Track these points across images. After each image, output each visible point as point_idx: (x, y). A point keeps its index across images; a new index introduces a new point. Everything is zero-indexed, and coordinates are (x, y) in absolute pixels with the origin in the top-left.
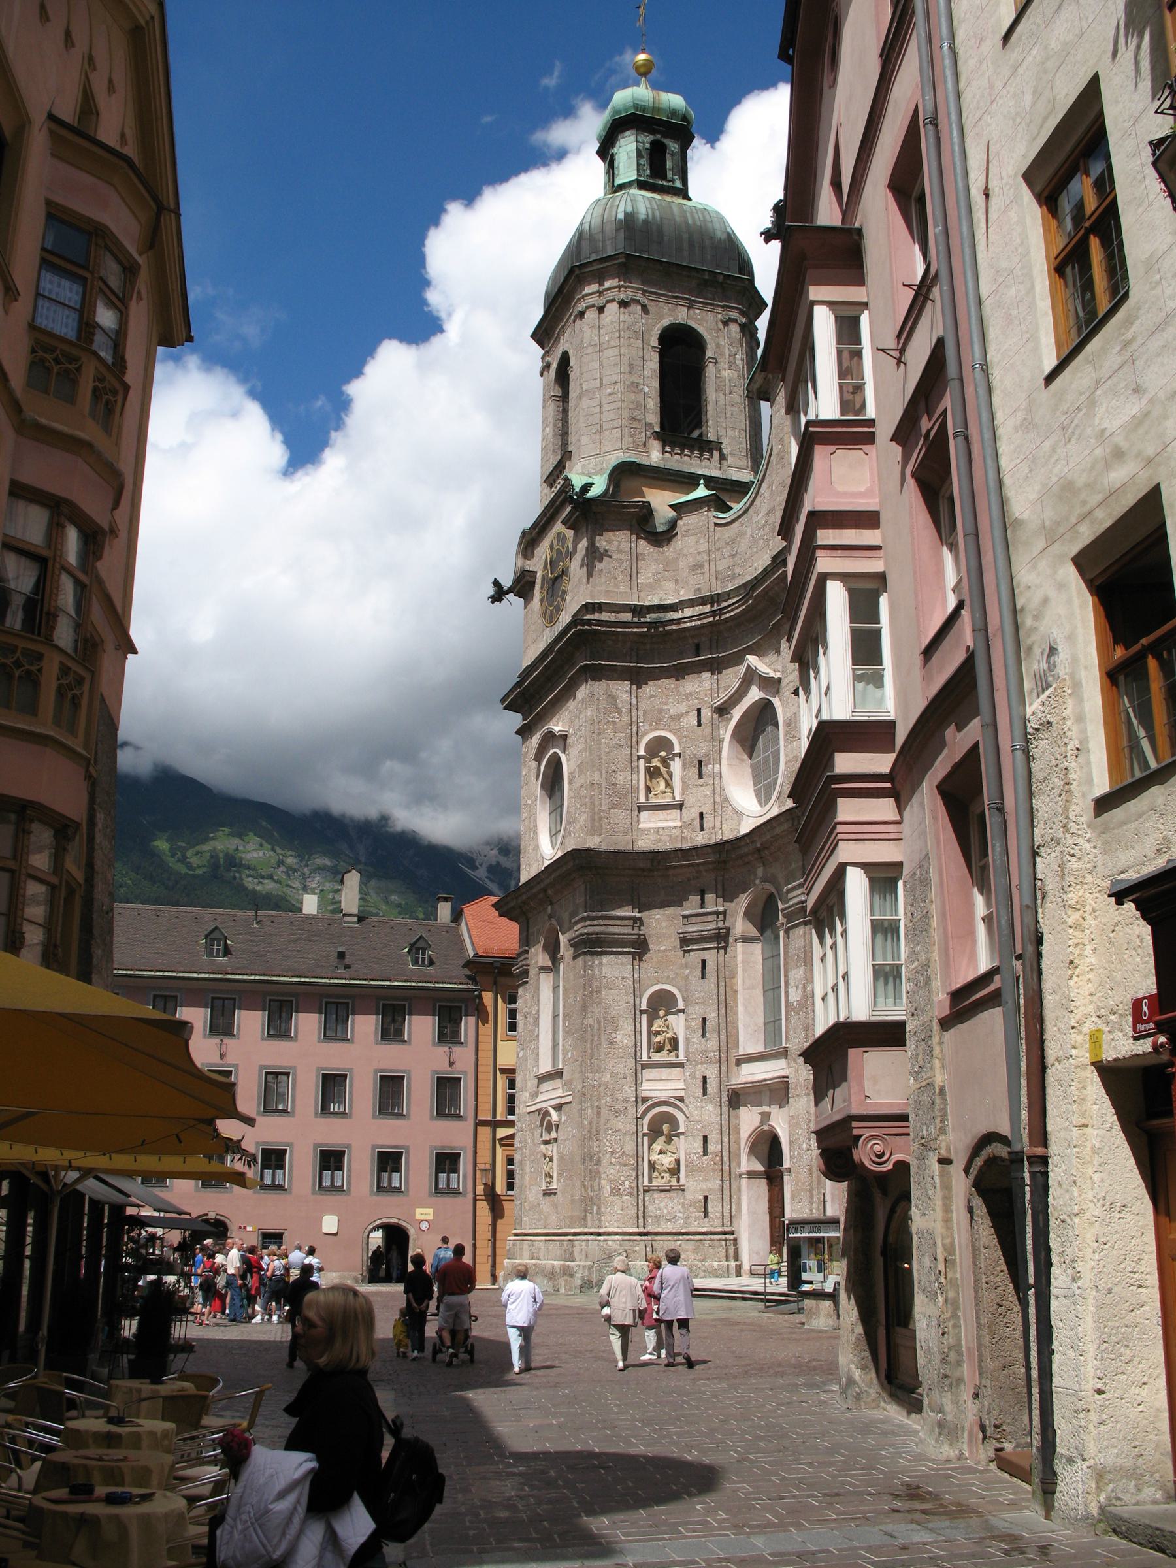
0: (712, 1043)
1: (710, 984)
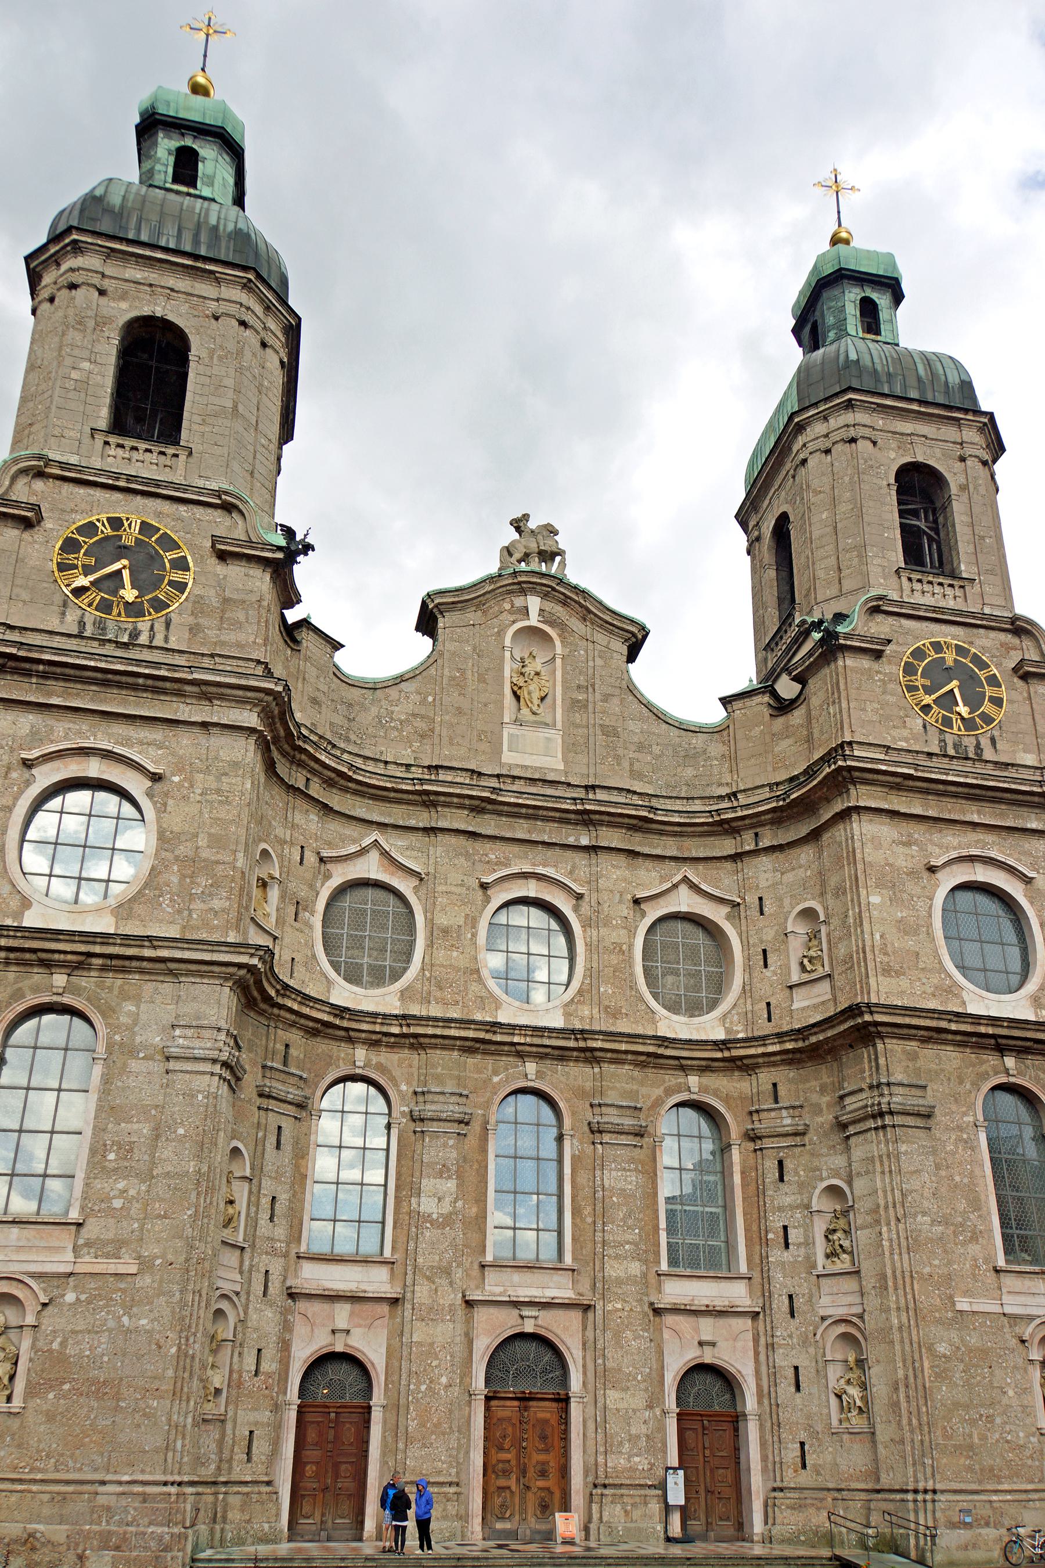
0: (280, 1231)
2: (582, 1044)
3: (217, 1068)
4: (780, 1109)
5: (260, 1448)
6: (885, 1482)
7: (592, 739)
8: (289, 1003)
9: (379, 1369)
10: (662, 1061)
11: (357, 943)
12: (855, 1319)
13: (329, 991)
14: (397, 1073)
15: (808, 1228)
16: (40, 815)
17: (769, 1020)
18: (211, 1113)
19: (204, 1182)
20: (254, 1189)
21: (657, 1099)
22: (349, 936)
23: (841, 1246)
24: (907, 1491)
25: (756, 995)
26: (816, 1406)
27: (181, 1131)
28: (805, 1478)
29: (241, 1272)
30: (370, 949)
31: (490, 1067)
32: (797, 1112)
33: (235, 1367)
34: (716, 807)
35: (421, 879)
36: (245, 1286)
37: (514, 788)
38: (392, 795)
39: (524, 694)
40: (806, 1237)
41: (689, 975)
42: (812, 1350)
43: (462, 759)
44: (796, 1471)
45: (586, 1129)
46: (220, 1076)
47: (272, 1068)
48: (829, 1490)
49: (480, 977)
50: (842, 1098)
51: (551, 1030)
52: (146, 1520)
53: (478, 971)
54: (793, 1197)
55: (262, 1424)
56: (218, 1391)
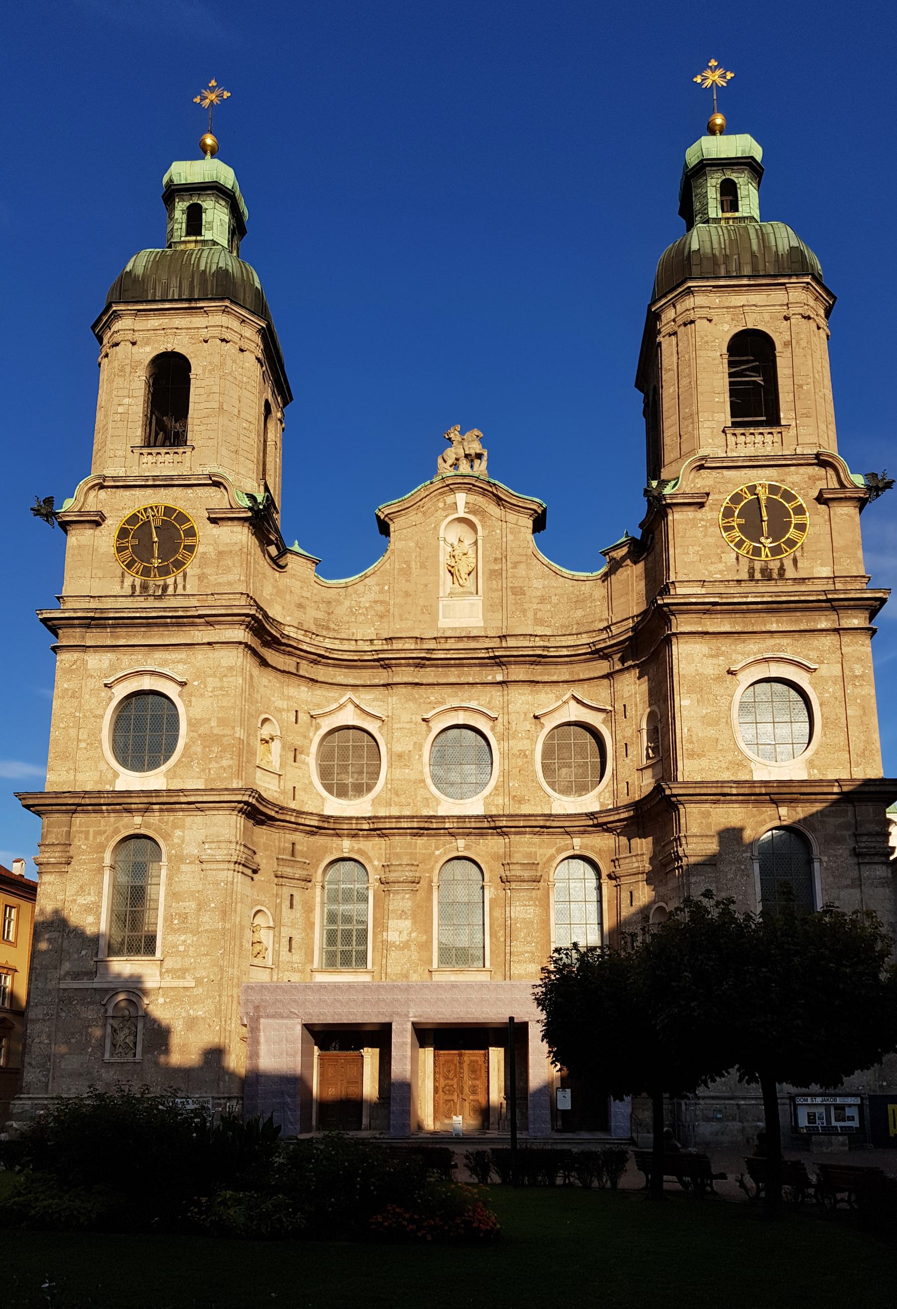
3: (232, 866)
22: (339, 765)
27: (213, 905)
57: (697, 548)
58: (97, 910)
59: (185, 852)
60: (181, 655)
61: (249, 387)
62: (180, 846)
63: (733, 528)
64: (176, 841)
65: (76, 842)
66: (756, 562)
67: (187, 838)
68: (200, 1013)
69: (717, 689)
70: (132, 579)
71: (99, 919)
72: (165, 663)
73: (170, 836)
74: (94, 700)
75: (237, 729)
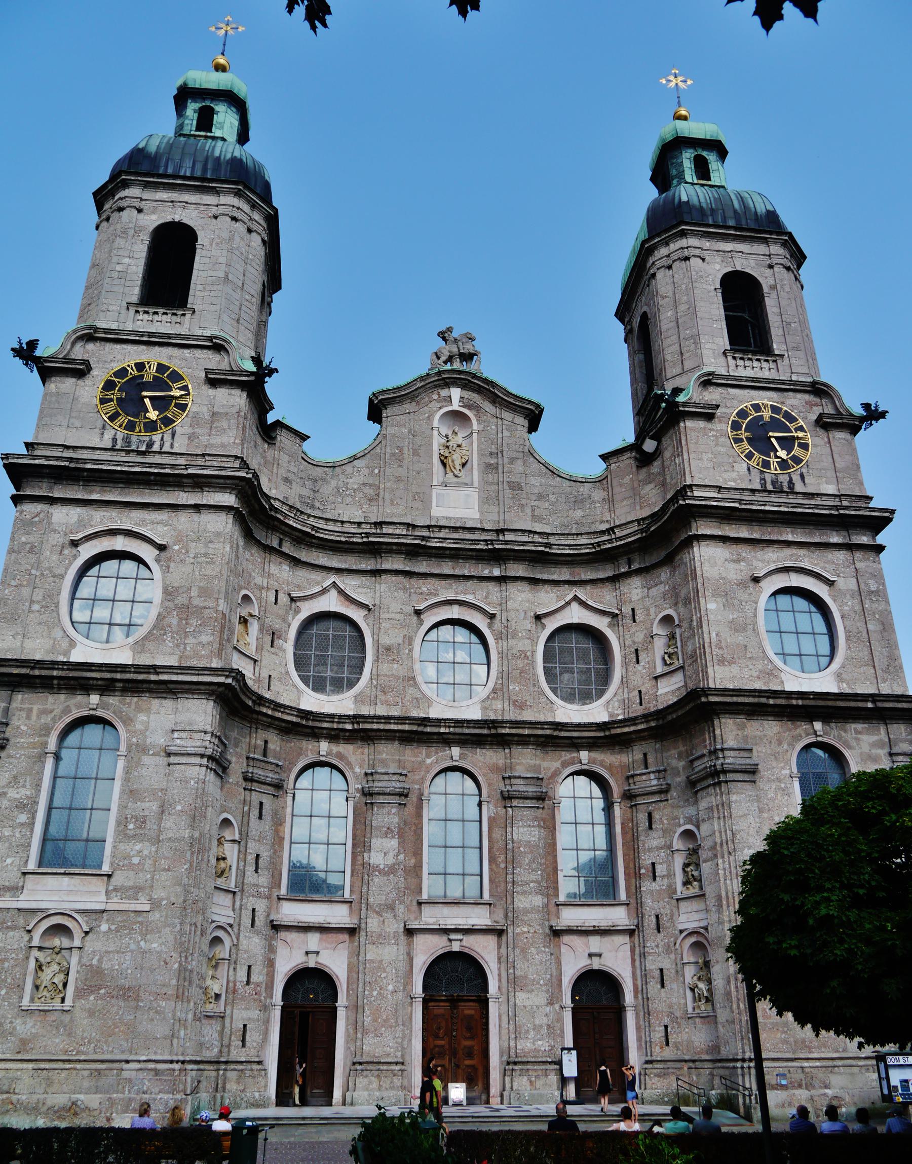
0: (263, 880)
1: (266, 825)
2: (493, 731)
3: (205, 761)
4: (649, 773)
5: (252, 1037)
6: (725, 1052)
7: (501, 493)
8: (264, 710)
9: (342, 980)
10: (558, 741)
11: (322, 661)
12: (702, 931)
13: (299, 699)
14: (352, 759)
15: (670, 864)
16: (85, 579)
17: (641, 704)
18: (201, 794)
19: (198, 846)
20: (242, 849)
21: (556, 771)
23: (693, 875)
24: (736, 1060)
25: (631, 686)
26: (676, 998)
27: (179, 808)
28: (668, 1053)
29: (234, 910)
30: (332, 665)
31: (424, 752)
32: (661, 775)
33: (231, 979)
34: (599, 540)
35: (370, 610)
36: (237, 920)
37: (441, 535)
38: (346, 546)
39: (449, 462)
40: (669, 870)
41: (581, 672)
42: (672, 956)
43: (401, 516)
44: (661, 1048)
45: (499, 796)
46: (207, 767)
47: (254, 759)
48: (686, 1061)
49: (415, 683)
50: (692, 762)
51: (469, 722)
52: (157, 1090)
53: (414, 678)
54: (659, 841)
55: (254, 1020)
56: (218, 996)
57: (710, 455)
58: (32, 807)
59: (149, 741)
60: (163, 516)
61: (254, 264)
62: (142, 733)
63: (741, 440)
64: (139, 727)
65: (15, 722)
66: (766, 475)
67: (152, 724)
68: (155, 945)
69: (741, 595)
70: (113, 432)
71: (34, 818)
72: (143, 523)
73: (131, 720)
74: (55, 557)
75: (221, 601)
